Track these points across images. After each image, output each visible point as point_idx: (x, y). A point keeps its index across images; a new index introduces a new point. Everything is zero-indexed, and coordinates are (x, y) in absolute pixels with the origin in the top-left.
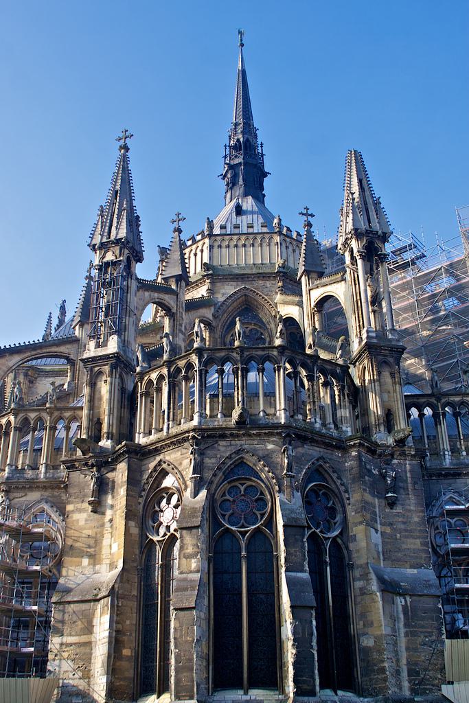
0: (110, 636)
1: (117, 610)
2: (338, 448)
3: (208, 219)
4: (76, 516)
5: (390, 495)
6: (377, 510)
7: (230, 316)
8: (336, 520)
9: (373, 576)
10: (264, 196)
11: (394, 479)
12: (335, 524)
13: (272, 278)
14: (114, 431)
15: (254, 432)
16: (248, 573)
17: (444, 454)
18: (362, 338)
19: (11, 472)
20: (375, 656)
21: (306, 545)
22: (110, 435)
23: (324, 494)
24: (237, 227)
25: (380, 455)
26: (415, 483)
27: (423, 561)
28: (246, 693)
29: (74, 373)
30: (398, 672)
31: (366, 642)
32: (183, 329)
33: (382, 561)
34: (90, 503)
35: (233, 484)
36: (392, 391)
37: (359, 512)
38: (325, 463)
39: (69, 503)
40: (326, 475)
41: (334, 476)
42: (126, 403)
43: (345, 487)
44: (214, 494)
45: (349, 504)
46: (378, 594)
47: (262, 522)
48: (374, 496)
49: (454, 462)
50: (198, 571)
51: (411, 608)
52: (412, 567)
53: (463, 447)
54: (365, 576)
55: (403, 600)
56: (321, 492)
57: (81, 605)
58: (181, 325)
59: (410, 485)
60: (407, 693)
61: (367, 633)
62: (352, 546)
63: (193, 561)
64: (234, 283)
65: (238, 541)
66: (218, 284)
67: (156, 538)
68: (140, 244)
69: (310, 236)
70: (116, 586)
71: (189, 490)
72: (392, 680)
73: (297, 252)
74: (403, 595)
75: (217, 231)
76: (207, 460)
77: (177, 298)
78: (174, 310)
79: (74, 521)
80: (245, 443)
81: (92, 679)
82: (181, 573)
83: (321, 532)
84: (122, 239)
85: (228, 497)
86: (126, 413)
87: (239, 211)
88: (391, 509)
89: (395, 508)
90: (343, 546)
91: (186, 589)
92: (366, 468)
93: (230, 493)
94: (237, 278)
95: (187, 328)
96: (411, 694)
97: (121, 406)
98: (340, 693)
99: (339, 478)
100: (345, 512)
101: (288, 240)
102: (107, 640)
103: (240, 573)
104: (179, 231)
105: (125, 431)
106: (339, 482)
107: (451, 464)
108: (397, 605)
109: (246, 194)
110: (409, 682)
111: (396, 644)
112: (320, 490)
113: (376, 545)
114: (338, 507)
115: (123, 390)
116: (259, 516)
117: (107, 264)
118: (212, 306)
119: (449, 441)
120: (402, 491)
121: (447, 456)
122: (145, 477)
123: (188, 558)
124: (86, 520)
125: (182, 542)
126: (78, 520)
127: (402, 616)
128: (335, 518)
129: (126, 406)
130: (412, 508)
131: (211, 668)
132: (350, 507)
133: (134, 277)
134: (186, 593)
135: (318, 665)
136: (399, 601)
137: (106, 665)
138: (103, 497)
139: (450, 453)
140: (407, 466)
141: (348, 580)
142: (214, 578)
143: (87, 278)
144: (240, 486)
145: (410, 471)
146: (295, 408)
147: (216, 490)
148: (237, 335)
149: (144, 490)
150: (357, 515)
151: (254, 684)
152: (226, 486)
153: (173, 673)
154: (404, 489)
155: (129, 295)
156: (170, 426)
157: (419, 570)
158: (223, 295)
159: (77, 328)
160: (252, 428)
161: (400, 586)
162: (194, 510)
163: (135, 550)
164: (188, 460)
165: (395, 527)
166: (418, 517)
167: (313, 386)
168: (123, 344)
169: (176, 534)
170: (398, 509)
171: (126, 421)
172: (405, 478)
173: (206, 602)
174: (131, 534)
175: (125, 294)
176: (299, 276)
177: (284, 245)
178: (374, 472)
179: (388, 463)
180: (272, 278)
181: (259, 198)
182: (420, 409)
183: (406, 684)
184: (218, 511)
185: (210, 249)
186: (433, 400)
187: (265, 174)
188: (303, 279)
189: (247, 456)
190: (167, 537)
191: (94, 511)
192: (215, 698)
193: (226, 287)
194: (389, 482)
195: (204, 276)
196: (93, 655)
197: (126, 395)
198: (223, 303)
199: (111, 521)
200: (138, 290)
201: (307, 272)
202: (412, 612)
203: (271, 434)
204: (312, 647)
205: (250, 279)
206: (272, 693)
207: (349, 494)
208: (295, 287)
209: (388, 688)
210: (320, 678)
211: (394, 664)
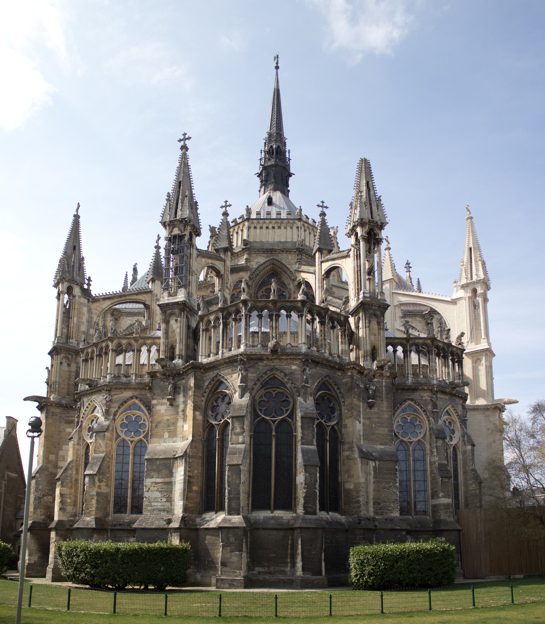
0: (185, 479)
1: (189, 464)
2: (339, 369)
3: (247, 206)
4: (158, 408)
5: (370, 400)
6: (361, 409)
7: (261, 278)
8: (335, 415)
9: (356, 449)
10: (289, 191)
11: (374, 391)
12: (334, 417)
13: (293, 252)
14: (183, 354)
15: (283, 357)
16: (276, 445)
17: (408, 377)
18: (359, 298)
19: (111, 378)
20: (354, 493)
21: (316, 429)
22: (181, 357)
23: (328, 398)
24: (269, 213)
25: (366, 376)
26: (387, 394)
27: (388, 441)
28: (272, 512)
29: (149, 314)
30: (367, 503)
31: (348, 486)
32: (229, 286)
33: (362, 441)
34: (168, 400)
35: (267, 391)
36: (377, 334)
37: (350, 411)
38: (330, 379)
39: (153, 399)
40: (330, 387)
41: (336, 387)
42: (191, 335)
43: (342, 395)
44: (255, 396)
45: (344, 405)
46: (358, 459)
47: (287, 414)
48: (360, 401)
49: (414, 382)
50: (243, 443)
51: (379, 468)
52: (381, 444)
53: (421, 373)
54: (351, 449)
55: (374, 465)
56: (326, 397)
57: (165, 461)
58: (227, 283)
59: (384, 395)
60: (371, 514)
61: (350, 482)
62: (343, 431)
63: (240, 437)
64: (265, 255)
65: (270, 425)
66: (253, 255)
67: (214, 423)
68: (199, 223)
69: (323, 223)
70: (188, 450)
71: (237, 394)
72: (363, 507)
73: (312, 235)
74: (374, 460)
75: (254, 216)
76: (250, 375)
77: (225, 264)
78: (222, 273)
79: (157, 410)
80: (276, 363)
81: (173, 502)
82: (232, 444)
83: (325, 422)
84: (186, 218)
85: (264, 398)
86: (191, 342)
87: (270, 202)
88: (371, 409)
89: (373, 408)
90: (338, 431)
91: (235, 454)
92: (356, 384)
93: (265, 396)
94: (267, 252)
95: (232, 285)
96: (374, 515)
97: (188, 337)
98: (330, 513)
99: (338, 389)
100: (340, 410)
101: (306, 225)
102: (182, 481)
103: (271, 445)
104: (226, 214)
105: (190, 354)
106: (338, 391)
107: (412, 382)
108: (370, 466)
109: (275, 190)
110: (374, 509)
111: (368, 487)
112: (325, 396)
113: (359, 431)
114: (337, 407)
115: (188, 327)
116: (285, 411)
117: (175, 237)
118: (248, 270)
119: (412, 368)
120: (378, 398)
121: (410, 378)
122: (206, 384)
123: (237, 435)
124: (166, 410)
125: (233, 425)
126: (160, 410)
127: (372, 472)
128: (334, 413)
129: (191, 338)
130: (384, 409)
131: (250, 498)
132: (344, 407)
133: (195, 247)
134: (235, 456)
135: (319, 499)
136: (371, 463)
137: (182, 495)
138: (177, 396)
139: (412, 376)
140: (384, 383)
141: (339, 451)
142: (254, 447)
143: (156, 247)
144: (273, 392)
145: (385, 386)
146: (311, 342)
147: (256, 394)
148: (272, 291)
149: (205, 392)
150: (349, 412)
151: (277, 508)
152: (263, 392)
153: (226, 501)
154: (380, 397)
155: (191, 260)
156: (224, 352)
157: (386, 446)
158: (257, 263)
159: (150, 283)
160: (282, 355)
161: (372, 455)
162: (241, 406)
163: (200, 429)
164: (237, 374)
165: (372, 420)
166: (388, 415)
167: (324, 328)
168: (189, 295)
169: (228, 420)
170: (375, 409)
171: (191, 347)
172: (381, 391)
173: (248, 461)
174: (197, 420)
175: (189, 259)
176: (314, 251)
177: (303, 229)
178: (361, 386)
179: (371, 380)
180: (293, 252)
181: (285, 192)
182: (394, 347)
183: (371, 509)
184: (257, 407)
185: (248, 229)
186: (404, 342)
187: (290, 175)
188: (317, 255)
189: (278, 373)
190: (222, 422)
191: (171, 405)
192: (253, 515)
193: (259, 257)
194: (371, 393)
195: (243, 249)
196: (173, 489)
197: (191, 330)
198: (257, 269)
199: (183, 411)
200: (198, 257)
201: (320, 250)
202: (379, 470)
203: (295, 359)
204: (316, 488)
205: (277, 252)
206: (289, 513)
207: (344, 399)
208: (309, 260)
209: (361, 512)
210: (319, 505)
211: (365, 499)
